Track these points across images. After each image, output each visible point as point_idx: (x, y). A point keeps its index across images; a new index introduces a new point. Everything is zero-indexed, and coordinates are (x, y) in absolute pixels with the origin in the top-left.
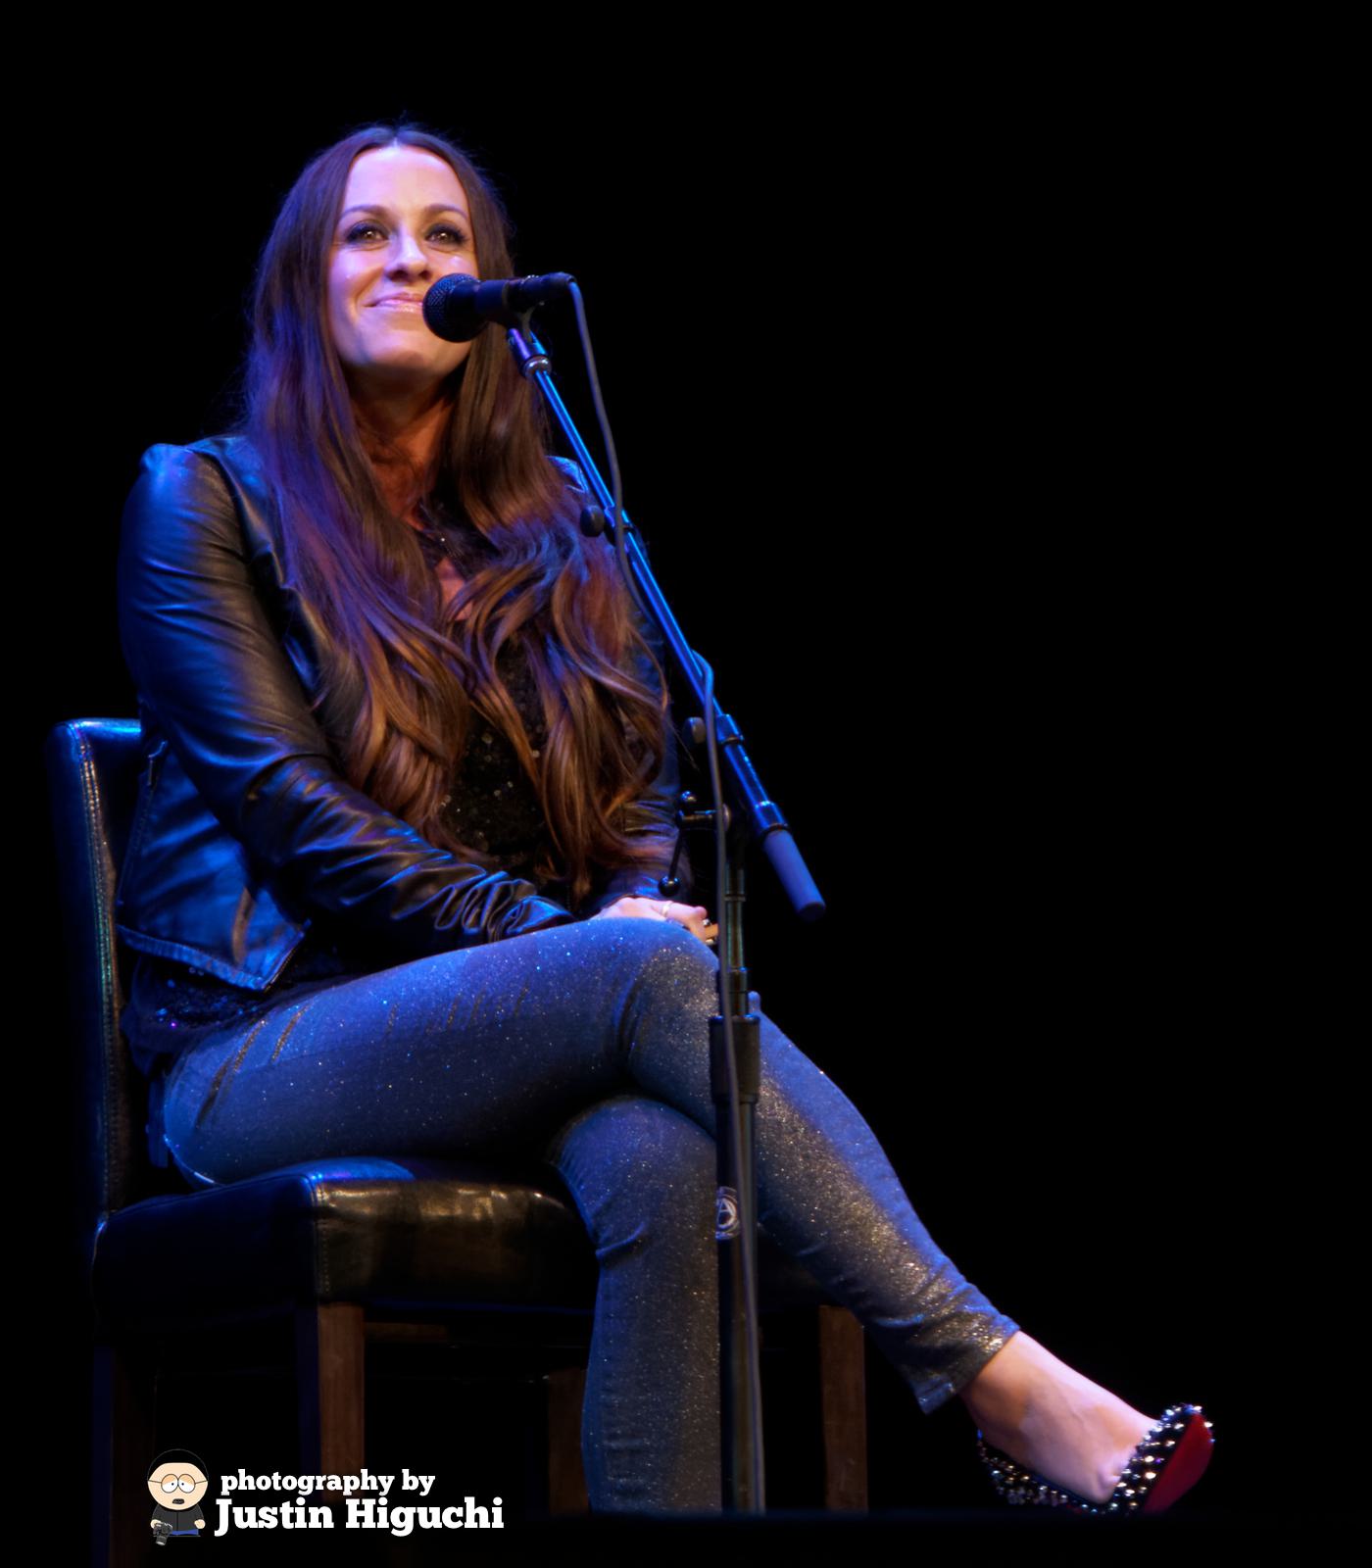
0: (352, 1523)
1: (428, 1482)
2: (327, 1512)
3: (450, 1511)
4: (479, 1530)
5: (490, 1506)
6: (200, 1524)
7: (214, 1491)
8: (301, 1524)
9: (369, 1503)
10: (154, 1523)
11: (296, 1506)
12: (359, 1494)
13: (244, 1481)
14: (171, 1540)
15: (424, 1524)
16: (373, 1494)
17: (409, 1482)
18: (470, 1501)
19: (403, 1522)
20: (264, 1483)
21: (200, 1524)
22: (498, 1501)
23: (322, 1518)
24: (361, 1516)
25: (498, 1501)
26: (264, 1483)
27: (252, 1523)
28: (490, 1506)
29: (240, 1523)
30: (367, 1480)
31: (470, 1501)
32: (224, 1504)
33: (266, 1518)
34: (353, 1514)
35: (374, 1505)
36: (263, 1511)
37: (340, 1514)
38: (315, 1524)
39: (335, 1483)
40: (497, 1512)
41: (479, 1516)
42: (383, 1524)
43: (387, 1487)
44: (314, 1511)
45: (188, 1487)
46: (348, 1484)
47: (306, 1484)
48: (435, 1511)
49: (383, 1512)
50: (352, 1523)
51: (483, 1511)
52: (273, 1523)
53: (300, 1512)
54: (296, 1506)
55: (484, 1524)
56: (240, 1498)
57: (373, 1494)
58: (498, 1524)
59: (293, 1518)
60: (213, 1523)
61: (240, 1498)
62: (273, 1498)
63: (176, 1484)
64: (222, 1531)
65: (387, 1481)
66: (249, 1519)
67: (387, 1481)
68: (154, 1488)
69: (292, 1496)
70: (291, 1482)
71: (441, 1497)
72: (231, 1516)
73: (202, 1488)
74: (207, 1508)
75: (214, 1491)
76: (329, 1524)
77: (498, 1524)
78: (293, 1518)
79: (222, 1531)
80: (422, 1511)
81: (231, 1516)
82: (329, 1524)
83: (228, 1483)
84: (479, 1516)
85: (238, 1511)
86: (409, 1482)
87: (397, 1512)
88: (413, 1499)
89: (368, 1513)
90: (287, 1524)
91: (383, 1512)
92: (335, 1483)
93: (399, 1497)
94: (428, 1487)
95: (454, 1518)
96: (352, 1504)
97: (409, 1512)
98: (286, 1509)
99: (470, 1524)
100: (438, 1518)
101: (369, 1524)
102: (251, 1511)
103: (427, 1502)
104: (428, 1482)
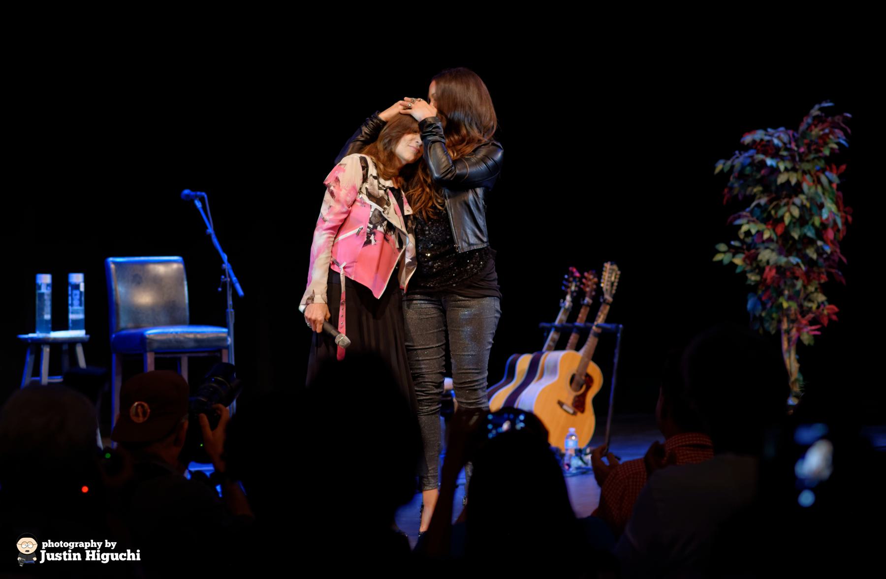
0: (88, 559)
1: (114, 544)
2: (79, 555)
5: (135, 553)
6: (35, 559)
7: (40, 547)
8: (70, 559)
9: (94, 552)
12: (90, 549)
13: (50, 544)
14: (25, 565)
15: (113, 559)
16: (95, 549)
17: (108, 544)
18: (129, 551)
19: (105, 558)
20: (57, 545)
21: (35, 559)
22: (138, 551)
23: (77, 557)
24: (91, 556)
25: (138, 551)
26: (57, 545)
27: (53, 559)
28: (135, 553)
29: (49, 559)
30: (93, 544)
31: (129, 551)
32: (43, 552)
33: (58, 557)
34: (88, 555)
35: (96, 552)
37: (84, 556)
38: (75, 559)
39: (82, 545)
40: (138, 555)
41: (131, 556)
42: (98, 559)
43: (100, 546)
44: (74, 555)
46: (87, 545)
47: (72, 545)
48: (117, 554)
49: (98, 555)
50: (88, 559)
51: (133, 554)
52: (60, 559)
53: (70, 555)
55: (134, 559)
56: (49, 550)
57: (95, 549)
58: (139, 559)
60: (39, 558)
61: (49, 550)
62: (60, 550)
63: (26, 545)
64: (42, 561)
65: (100, 544)
66: (51, 557)
67: (100, 544)
68: (19, 546)
69: (67, 549)
70: (66, 545)
71: (118, 550)
72: (46, 556)
74: (37, 553)
75: (40, 547)
76: (80, 559)
77: (139, 559)
79: (42, 561)
80: (112, 555)
81: (46, 556)
82: (80, 559)
83: (45, 545)
84: (131, 556)
85: (48, 555)
86: (108, 544)
87: (103, 555)
88: (109, 550)
89: (93, 555)
90: (65, 559)
91: (98, 555)
92: (82, 545)
93: (104, 550)
94: (114, 546)
95: (123, 557)
96: (88, 552)
97: (108, 555)
98: (65, 554)
99: (129, 559)
100: (118, 557)
103: (114, 551)
104: (114, 544)
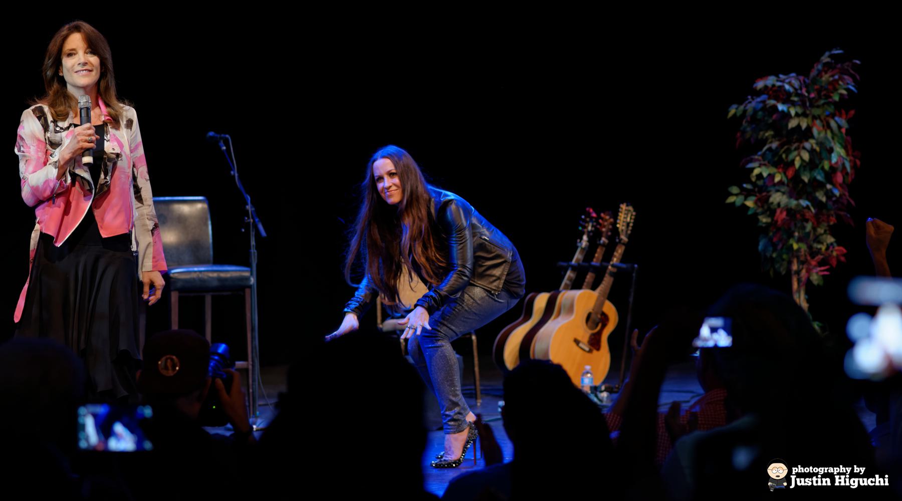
0: (837, 484)
1: (863, 470)
2: (828, 480)
3: (870, 480)
4: (822, 486)
5: (884, 478)
6: (785, 484)
7: (790, 473)
8: (819, 484)
9: (843, 477)
10: (769, 484)
11: (817, 478)
12: (839, 474)
13: (800, 469)
14: (775, 490)
15: (862, 484)
17: (857, 470)
18: (877, 476)
19: (854, 483)
20: (807, 470)
21: (785, 484)
23: (827, 482)
24: (840, 481)
26: (807, 470)
27: (803, 484)
28: (884, 478)
29: (799, 484)
30: (842, 469)
31: (877, 476)
32: (793, 477)
33: (808, 482)
34: (837, 480)
35: (846, 478)
36: (807, 480)
37: (833, 481)
38: (824, 484)
39: (831, 470)
40: (887, 480)
41: (880, 481)
42: (847, 484)
44: (824, 480)
45: (781, 471)
46: (836, 470)
47: (822, 470)
48: (865, 480)
49: (847, 480)
50: (837, 484)
51: (882, 480)
52: (810, 484)
53: (819, 480)
54: (817, 478)
55: (882, 484)
56: (799, 475)
58: (887, 484)
59: (817, 482)
60: (790, 483)
61: (799, 475)
62: (810, 475)
63: (777, 471)
64: (793, 486)
65: (849, 470)
66: (802, 482)
67: (849, 470)
68: (769, 472)
69: (816, 474)
70: (816, 470)
71: (867, 475)
73: (786, 471)
74: (788, 478)
75: (790, 473)
76: (829, 484)
77: (887, 484)
78: (817, 482)
79: (793, 486)
80: (861, 480)
82: (829, 484)
83: (795, 470)
84: (880, 481)
85: (798, 480)
86: (857, 470)
87: (852, 480)
88: (857, 475)
90: (815, 484)
91: (847, 480)
92: (831, 470)
93: (853, 475)
96: (837, 477)
97: (856, 480)
98: (814, 479)
99: (877, 484)
101: (843, 484)
102: (802, 480)
103: (862, 477)
104: (863, 470)
